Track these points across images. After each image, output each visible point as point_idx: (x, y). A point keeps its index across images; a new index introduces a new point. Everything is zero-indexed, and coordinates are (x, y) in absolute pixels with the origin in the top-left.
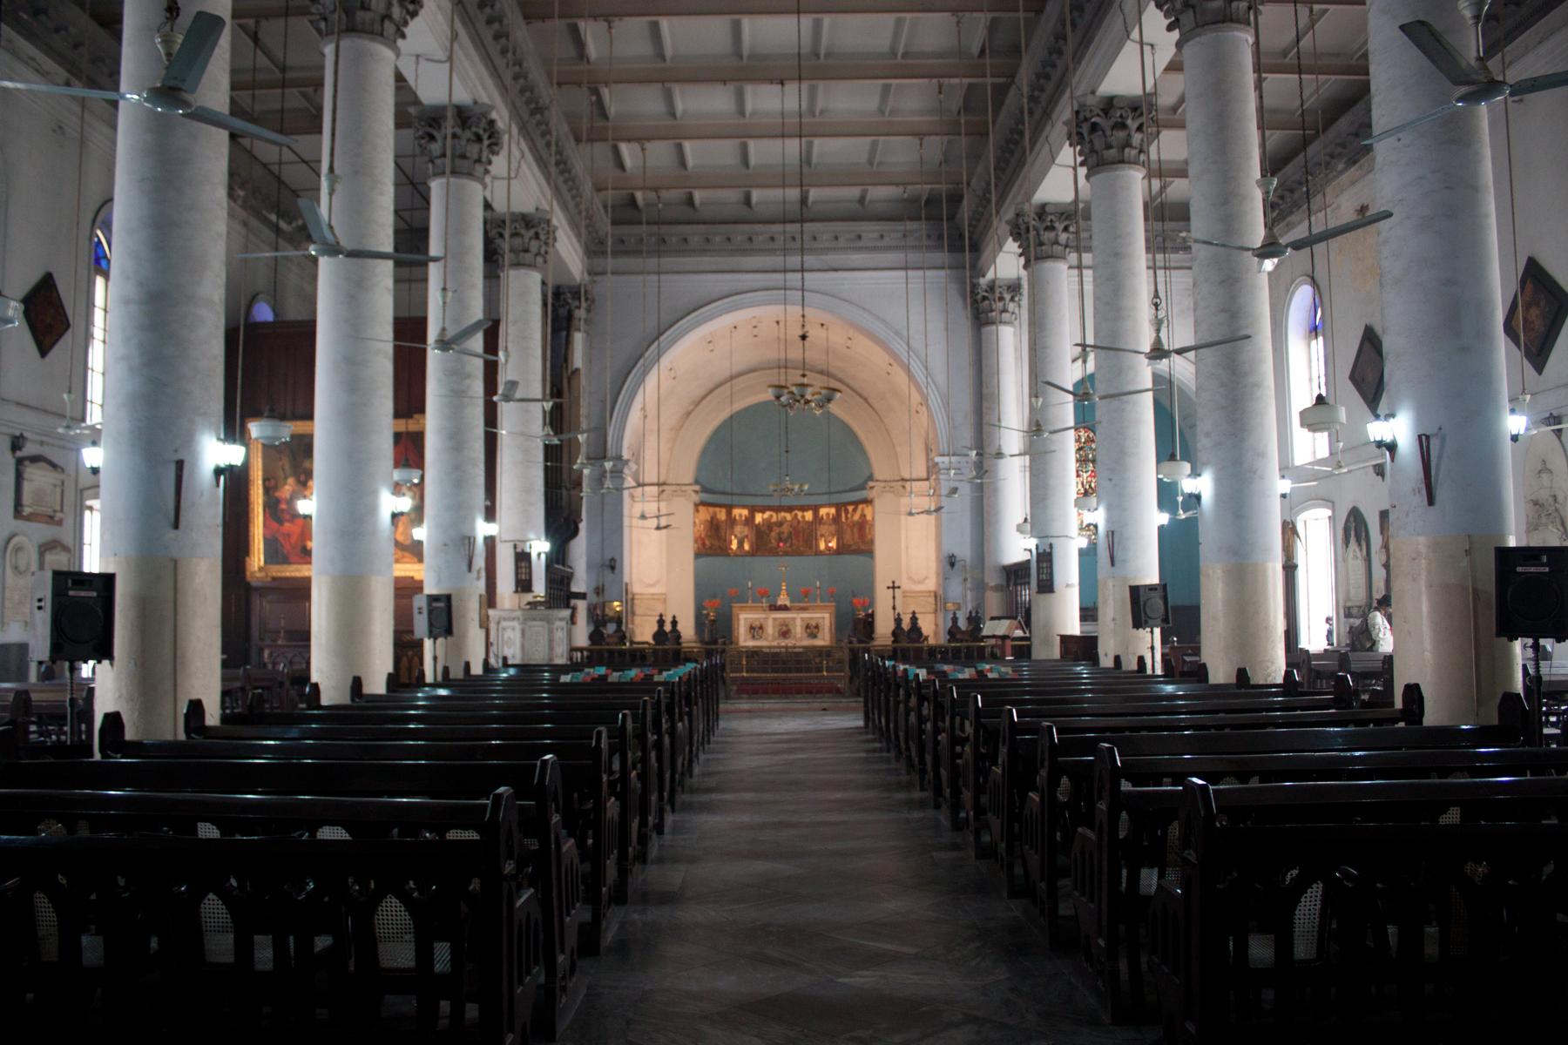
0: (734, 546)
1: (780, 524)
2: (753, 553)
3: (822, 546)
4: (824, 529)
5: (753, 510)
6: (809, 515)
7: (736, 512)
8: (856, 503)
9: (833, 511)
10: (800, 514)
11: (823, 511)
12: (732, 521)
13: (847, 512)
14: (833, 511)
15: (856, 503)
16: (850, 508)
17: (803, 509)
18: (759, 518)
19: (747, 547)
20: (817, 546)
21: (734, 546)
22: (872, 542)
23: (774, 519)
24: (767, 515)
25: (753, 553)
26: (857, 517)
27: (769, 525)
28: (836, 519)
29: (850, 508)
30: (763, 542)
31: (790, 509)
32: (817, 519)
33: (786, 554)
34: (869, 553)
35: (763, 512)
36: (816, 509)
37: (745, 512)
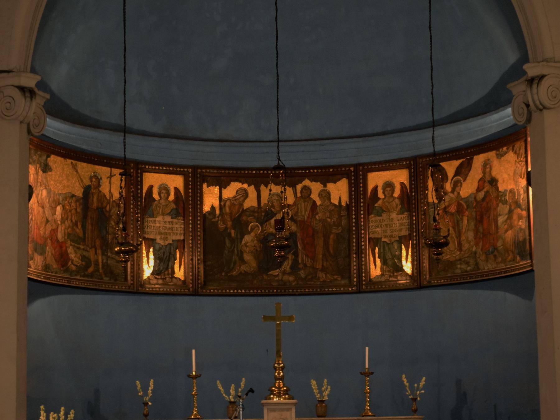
0: (148, 270)
1: (263, 214)
2: (194, 289)
3: (375, 270)
4: (376, 226)
5: (197, 177)
6: (339, 191)
7: (152, 180)
8: (466, 153)
9: (400, 177)
10: (316, 187)
11: (376, 179)
12: (139, 203)
13: (441, 176)
14: (400, 177)
15: (466, 153)
16: (450, 167)
17: (327, 174)
18: (211, 198)
19: (179, 274)
20: (362, 268)
21: (148, 270)
22: (524, 249)
23: (251, 202)
24: (230, 192)
25: (194, 289)
26: (468, 188)
27: (238, 217)
28: (411, 200)
29: (450, 167)
30: (222, 260)
31: (290, 176)
32: (363, 202)
33: (284, 290)
34: (522, 282)
35: (223, 185)
36: (356, 174)
37: (176, 182)
